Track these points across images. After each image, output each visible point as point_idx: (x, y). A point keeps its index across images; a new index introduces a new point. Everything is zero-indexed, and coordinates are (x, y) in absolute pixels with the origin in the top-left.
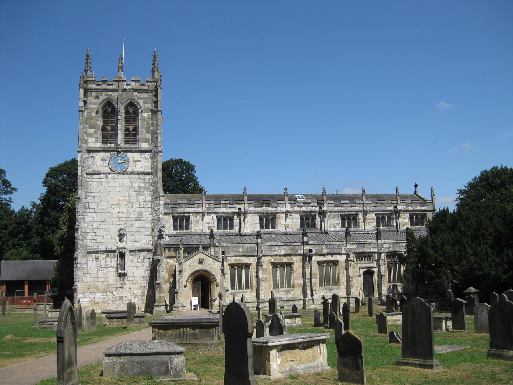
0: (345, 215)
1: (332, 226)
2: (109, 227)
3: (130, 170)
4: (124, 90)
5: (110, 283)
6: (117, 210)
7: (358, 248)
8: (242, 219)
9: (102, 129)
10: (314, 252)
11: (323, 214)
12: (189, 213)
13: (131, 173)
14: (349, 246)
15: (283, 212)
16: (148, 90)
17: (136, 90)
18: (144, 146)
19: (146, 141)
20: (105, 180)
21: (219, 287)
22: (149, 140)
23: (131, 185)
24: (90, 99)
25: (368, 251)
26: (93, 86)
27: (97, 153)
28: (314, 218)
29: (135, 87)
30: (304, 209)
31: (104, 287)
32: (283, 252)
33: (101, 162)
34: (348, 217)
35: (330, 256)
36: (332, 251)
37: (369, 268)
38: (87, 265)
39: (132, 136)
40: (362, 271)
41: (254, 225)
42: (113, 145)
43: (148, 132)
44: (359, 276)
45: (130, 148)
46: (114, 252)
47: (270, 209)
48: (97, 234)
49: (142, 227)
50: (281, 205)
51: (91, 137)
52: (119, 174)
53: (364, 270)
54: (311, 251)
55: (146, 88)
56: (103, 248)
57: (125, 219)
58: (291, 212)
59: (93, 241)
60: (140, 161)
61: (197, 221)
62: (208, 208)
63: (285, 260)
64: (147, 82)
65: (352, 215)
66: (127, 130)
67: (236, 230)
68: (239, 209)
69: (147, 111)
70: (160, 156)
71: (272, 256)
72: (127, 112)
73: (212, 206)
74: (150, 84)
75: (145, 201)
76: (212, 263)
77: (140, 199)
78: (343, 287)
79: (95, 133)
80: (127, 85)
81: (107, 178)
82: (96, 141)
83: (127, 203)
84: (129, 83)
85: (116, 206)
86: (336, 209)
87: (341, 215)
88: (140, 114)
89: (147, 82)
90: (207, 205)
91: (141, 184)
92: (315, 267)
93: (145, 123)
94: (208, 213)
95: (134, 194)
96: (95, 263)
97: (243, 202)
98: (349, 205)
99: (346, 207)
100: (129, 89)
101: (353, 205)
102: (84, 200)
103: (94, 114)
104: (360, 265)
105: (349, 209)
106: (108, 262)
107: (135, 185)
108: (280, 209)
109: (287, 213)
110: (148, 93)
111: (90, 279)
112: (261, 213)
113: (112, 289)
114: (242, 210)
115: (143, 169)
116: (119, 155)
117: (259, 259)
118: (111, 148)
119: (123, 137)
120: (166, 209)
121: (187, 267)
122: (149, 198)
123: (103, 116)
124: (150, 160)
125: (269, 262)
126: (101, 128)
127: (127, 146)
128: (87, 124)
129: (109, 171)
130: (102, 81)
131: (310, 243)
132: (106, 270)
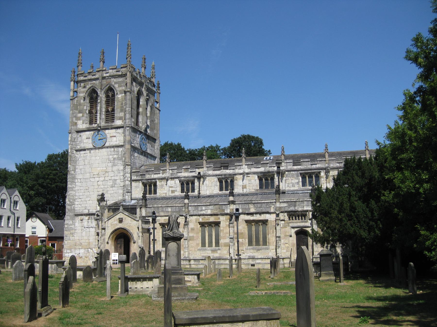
0: (307, 173)
1: (291, 185)
2: (91, 193)
3: (107, 144)
4: (104, 78)
5: (91, 241)
6: (97, 179)
7: (289, 206)
8: (201, 182)
9: (89, 113)
10: (240, 211)
11: (280, 174)
12: (155, 179)
13: (107, 147)
14: (278, 205)
15: (241, 174)
16: (122, 75)
17: (113, 76)
18: (118, 123)
19: (120, 118)
20: (89, 154)
21: (136, 244)
22: (122, 117)
23: (107, 157)
24: (81, 89)
25: (300, 209)
26: (82, 78)
27: (84, 133)
28: (273, 179)
29: (112, 74)
30: (262, 169)
31: (86, 244)
32: (209, 212)
33: (86, 140)
34: (310, 175)
35: (258, 215)
36: (260, 210)
37: (302, 227)
38: (75, 226)
39: (110, 116)
40: (293, 231)
41: (213, 188)
42: (96, 125)
43: (121, 111)
44: (291, 236)
45: (108, 126)
47: (228, 172)
49: (116, 193)
50: (239, 167)
51: (80, 120)
52: (99, 148)
53: (296, 229)
54: (237, 210)
55: (120, 73)
56: (86, 212)
57: (102, 187)
58: (248, 174)
59: (79, 206)
60: (115, 136)
61: (162, 186)
62: (172, 174)
63: (212, 219)
64: (122, 68)
65: (314, 173)
66: (107, 111)
67: (196, 193)
68: (199, 173)
69: (121, 93)
70: (128, 130)
71: (199, 215)
72: (107, 96)
73: (175, 171)
74: (124, 69)
75: (119, 170)
76: (130, 222)
77: (115, 168)
78: (273, 247)
79: (83, 116)
80: (106, 73)
81: (90, 152)
82: (83, 123)
83: (104, 173)
84: (108, 71)
85: (97, 176)
86: (295, 167)
87: (301, 174)
88: (116, 96)
89: (122, 68)
90: (171, 171)
91: (115, 156)
92: (243, 227)
93: (120, 103)
94: (171, 178)
95: (110, 164)
96: (80, 224)
97: (202, 166)
98: (310, 163)
99: (306, 165)
100: (108, 77)
101: (314, 163)
102: (73, 172)
103: (82, 101)
104: (291, 225)
105: (309, 167)
106: (90, 223)
107: (111, 157)
108: (237, 171)
109: (243, 174)
110: (122, 77)
111: (76, 237)
112: (219, 175)
113: (92, 246)
114: (202, 174)
115: (117, 143)
116: (99, 133)
117: (186, 218)
118: (93, 128)
119: (103, 117)
120: (137, 176)
121: (109, 225)
122: (122, 168)
123: (90, 102)
124: (123, 135)
125: (196, 221)
126: (87, 112)
127: (107, 125)
128: (77, 109)
129: (92, 147)
130: (89, 73)
131: (236, 203)
132: (88, 229)
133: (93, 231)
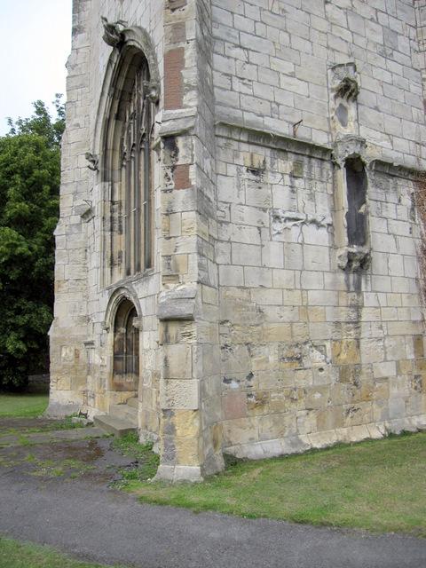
5: (314, 296)
31: (287, 315)
46: (323, 153)
48: (254, 57)
56: (282, 128)
59: (237, 85)
106: (302, 195)
133: (320, 248)
